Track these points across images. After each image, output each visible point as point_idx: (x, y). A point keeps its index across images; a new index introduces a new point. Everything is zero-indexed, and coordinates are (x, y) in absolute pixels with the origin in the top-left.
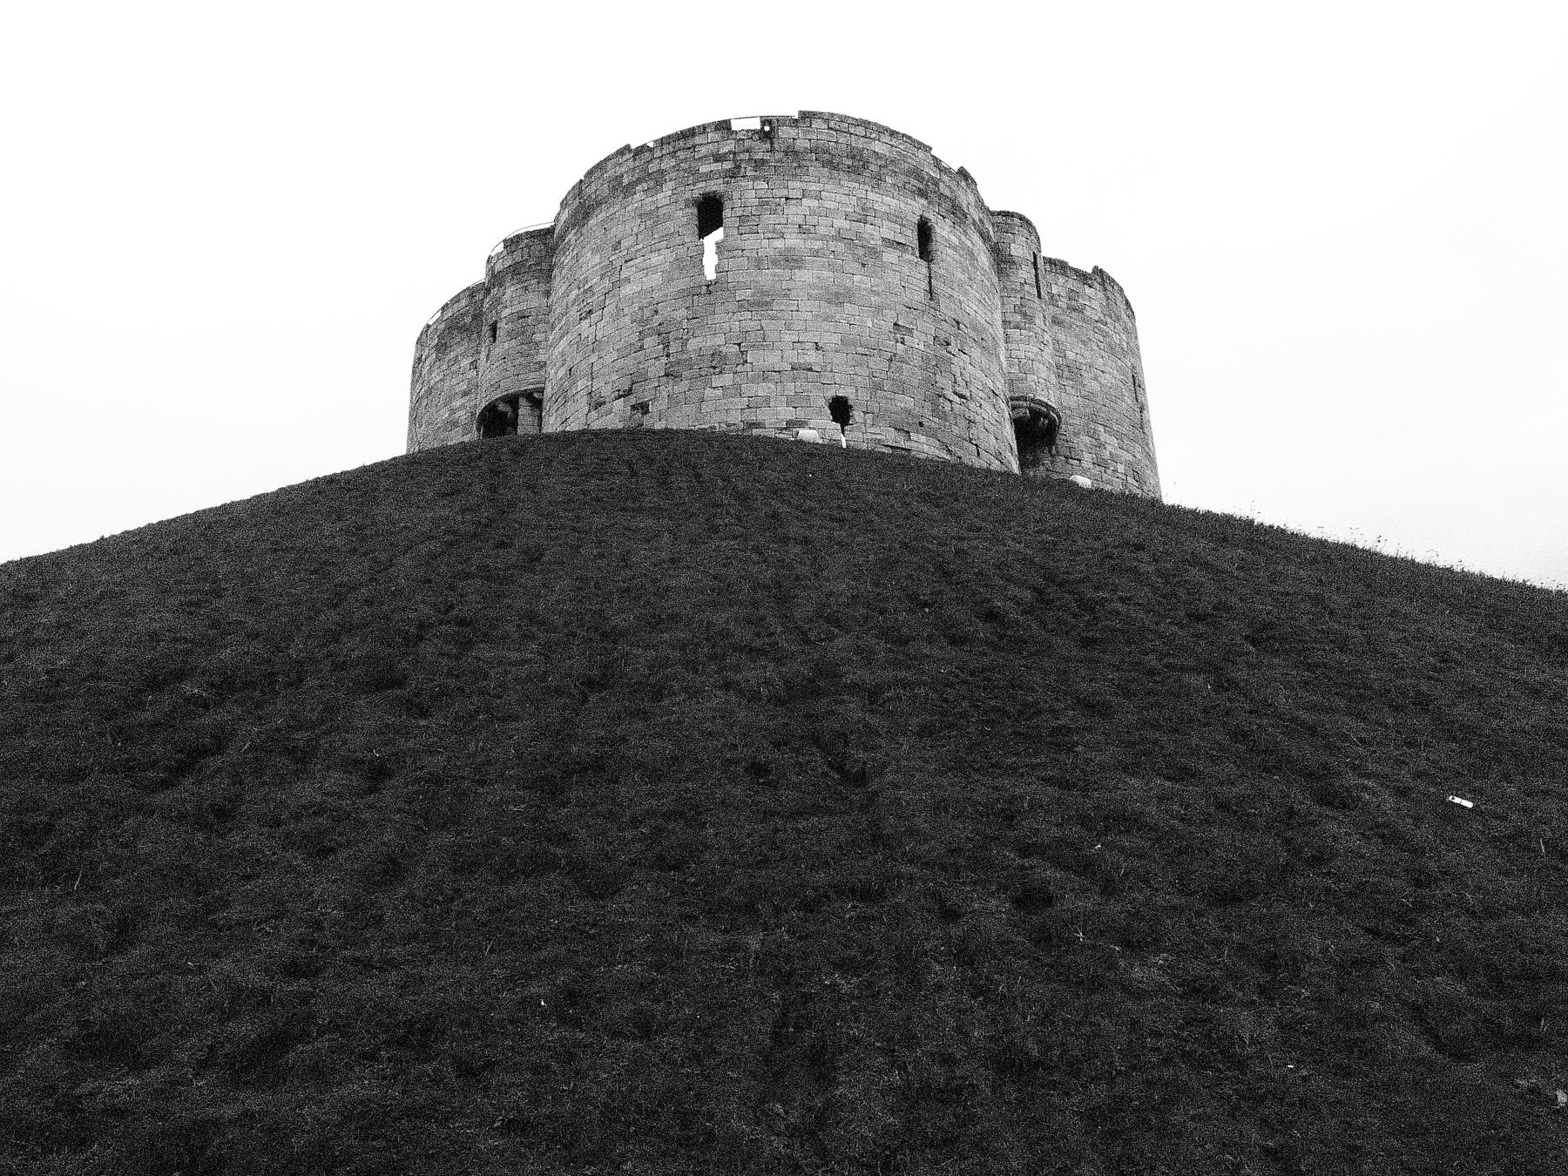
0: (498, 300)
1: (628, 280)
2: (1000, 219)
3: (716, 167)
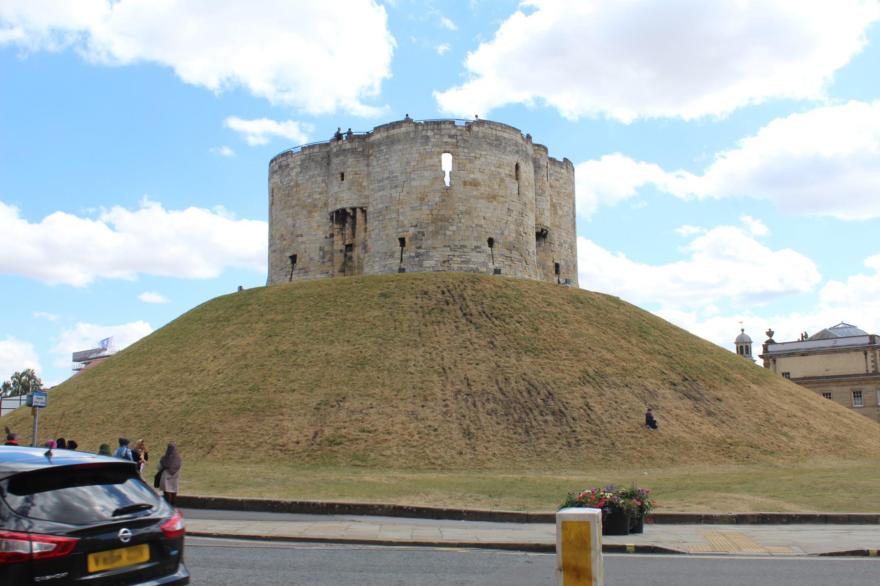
0: (345, 163)
1: (414, 179)
2: (536, 148)
3: (450, 140)
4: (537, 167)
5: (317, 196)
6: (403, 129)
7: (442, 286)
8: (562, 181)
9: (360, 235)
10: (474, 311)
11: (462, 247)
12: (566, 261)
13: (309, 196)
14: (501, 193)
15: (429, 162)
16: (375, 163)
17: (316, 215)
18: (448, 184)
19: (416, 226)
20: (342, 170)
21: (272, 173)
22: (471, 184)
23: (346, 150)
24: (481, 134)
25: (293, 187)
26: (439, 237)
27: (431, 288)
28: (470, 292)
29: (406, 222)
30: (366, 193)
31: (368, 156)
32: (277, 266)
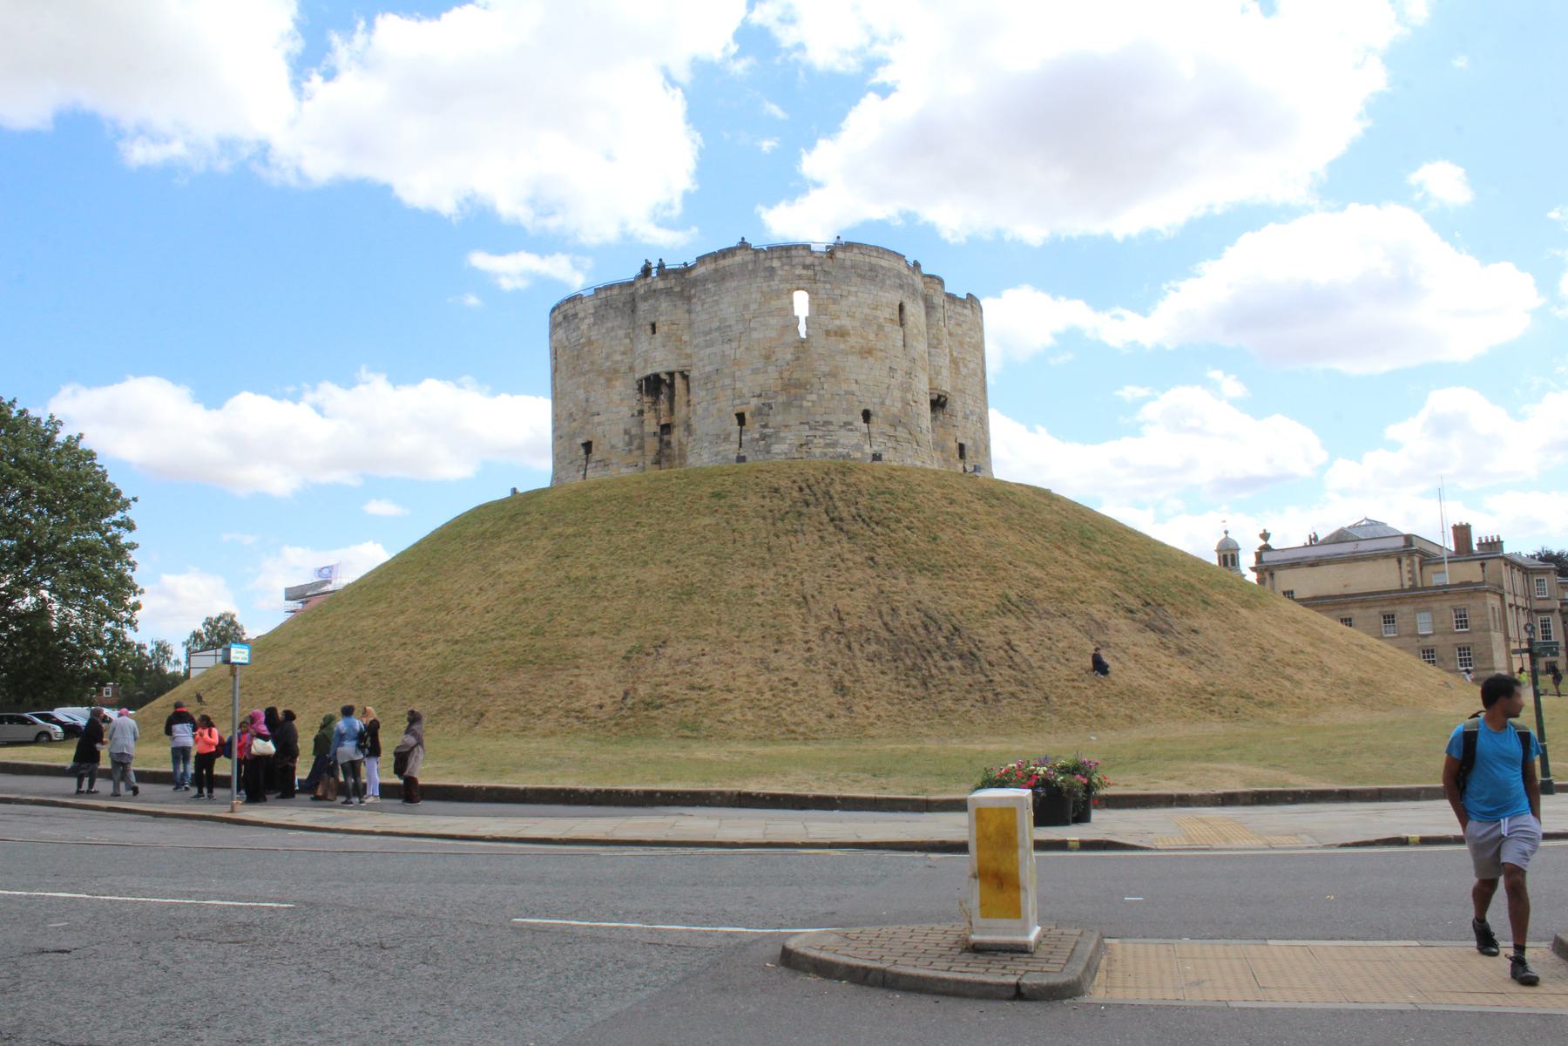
3: (804, 272)
4: (930, 307)
5: (618, 357)
6: (738, 258)
7: (799, 479)
8: (965, 327)
9: (681, 411)
10: (845, 515)
11: (827, 423)
12: (974, 440)
13: (608, 357)
14: (880, 345)
15: (775, 304)
16: (699, 308)
17: (617, 383)
18: (803, 335)
20: (653, 320)
21: (554, 326)
22: (836, 334)
23: (657, 290)
24: (848, 263)
25: (583, 345)
27: (784, 483)
28: (838, 487)
29: (745, 391)
30: (688, 351)
31: (689, 299)
32: (564, 458)
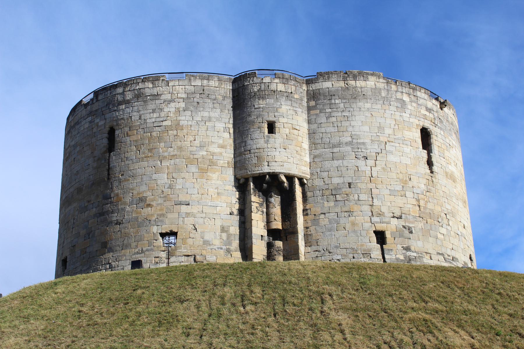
1: (391, 152)
3: (427, 113)
13: (201, 147)
19: (400, 217)
20: (271, 119)
26: (431, 239)
29: (384, 209)
